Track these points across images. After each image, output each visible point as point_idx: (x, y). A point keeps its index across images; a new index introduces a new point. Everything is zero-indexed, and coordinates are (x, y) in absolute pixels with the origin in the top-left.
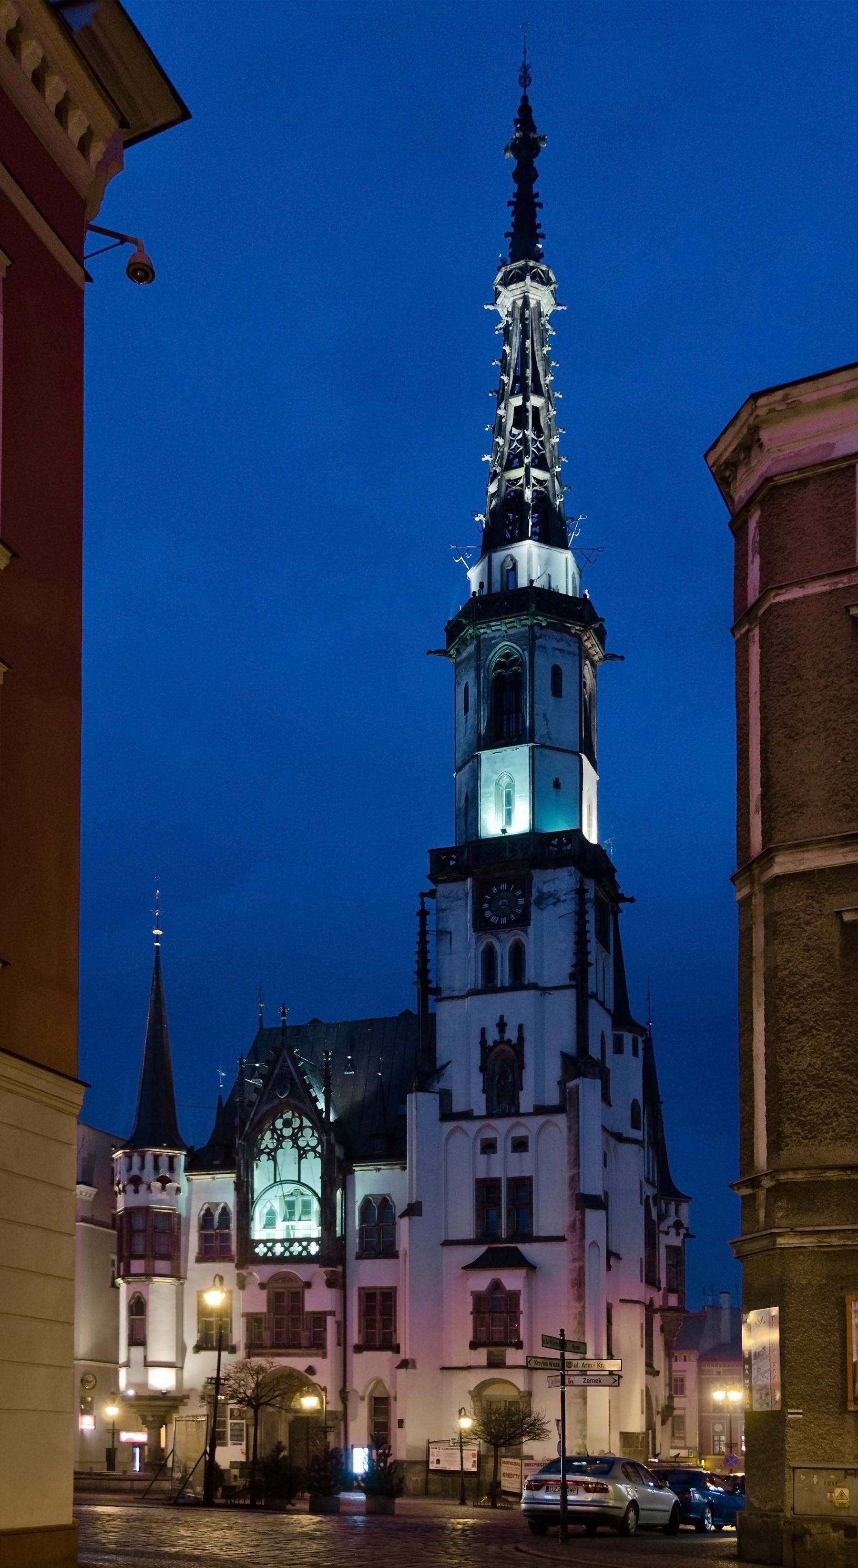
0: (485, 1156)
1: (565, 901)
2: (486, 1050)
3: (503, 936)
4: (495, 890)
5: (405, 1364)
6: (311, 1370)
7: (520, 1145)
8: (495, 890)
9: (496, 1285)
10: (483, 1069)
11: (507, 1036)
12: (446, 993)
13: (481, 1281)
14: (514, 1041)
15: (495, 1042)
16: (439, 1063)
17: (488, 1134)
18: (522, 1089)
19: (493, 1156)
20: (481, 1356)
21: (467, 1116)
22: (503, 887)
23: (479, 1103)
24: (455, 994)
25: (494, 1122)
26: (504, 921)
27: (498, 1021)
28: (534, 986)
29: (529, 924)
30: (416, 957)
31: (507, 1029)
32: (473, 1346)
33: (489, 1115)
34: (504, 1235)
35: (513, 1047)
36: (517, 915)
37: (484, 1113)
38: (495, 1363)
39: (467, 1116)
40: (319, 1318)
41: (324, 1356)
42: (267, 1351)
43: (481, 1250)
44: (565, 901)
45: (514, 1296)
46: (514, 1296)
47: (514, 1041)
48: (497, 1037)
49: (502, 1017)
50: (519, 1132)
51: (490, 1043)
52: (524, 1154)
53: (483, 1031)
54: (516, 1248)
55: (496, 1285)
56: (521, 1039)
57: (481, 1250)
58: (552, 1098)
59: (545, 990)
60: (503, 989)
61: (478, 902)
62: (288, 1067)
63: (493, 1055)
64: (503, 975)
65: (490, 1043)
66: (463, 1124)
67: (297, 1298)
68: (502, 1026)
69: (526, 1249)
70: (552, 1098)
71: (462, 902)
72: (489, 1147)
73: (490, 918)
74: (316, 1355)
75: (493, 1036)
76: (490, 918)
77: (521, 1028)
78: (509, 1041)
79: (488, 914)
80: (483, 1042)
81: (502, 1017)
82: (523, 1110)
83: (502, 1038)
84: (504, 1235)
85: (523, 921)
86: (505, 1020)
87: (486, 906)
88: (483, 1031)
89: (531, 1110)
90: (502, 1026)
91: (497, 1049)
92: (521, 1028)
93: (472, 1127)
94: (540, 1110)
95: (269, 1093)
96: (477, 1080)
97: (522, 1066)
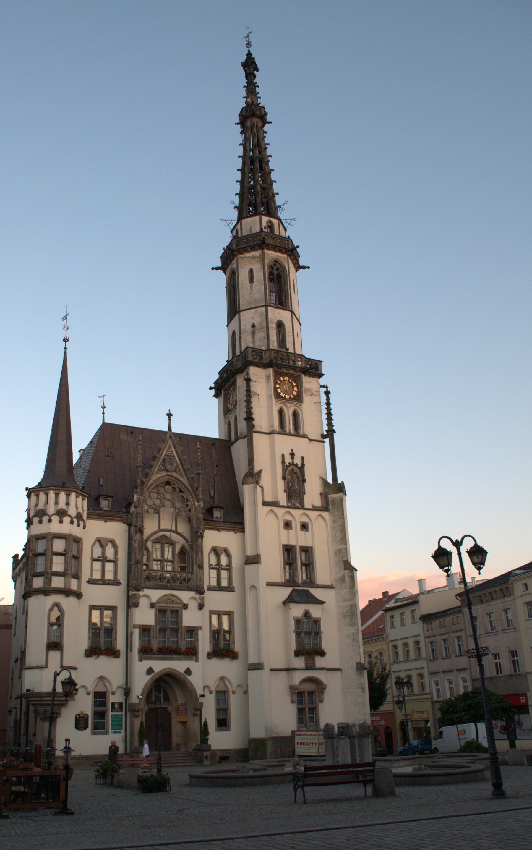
0: (286, 531)
1: (316, 395)
2: (285, 467)
3: (289, 405)
4: (282, 379)
5: (258, 667)
6: (188, 671)
7: (304, 527)
8: (282, 379)
9: (307, 614)
10: (284, 478)
11: (295, 463)
12: (257, 429)
13: (297, 610)
14: (299, 465)
15: (289, 463)
16: (256, 469)
17: (288, 518)
18: (305, 493)
19: (290, 531)
20: (300, 662)
21: (275, 504)
22: (286, 378)
23: (283, 498)
24: (263, 431)
25: (292, 511)
26: (287, 397)
27: (290, 452)
28: (304, 436)
29: (302, 402)
30: (245, 404)
31: (295, 457)
32: (297, 654)
33: (288, 507)
34: (300, 581)
35: (299, 468)
36: (294, 396)
37: (285, 504)
38: (310, 667)
39: (275, 504)
40: (193, 631)
41: (197, 660)
42: (155, 656)
43: (288, 590)
44: (316, 395)
45: (317, 622)
46: (317, 622)
47: (299, 465)
48: (290, 461)
49: (292, 450)
50: (305, 519)
51: (287, 464)
52: (306, 532)
53: (283, 455)
54: (308, 591)
55: (307, 614)
56: (303, 465)
57: (289, 590)
58: (318, 503)
59: (310, 440)
60: (290, 434)
61: (275, 383)
62: (172, 452)
63: (288, 471)
64: (290, 426)
65: (287, 464)
66: (275, 509)
67: (176, 613)
68: (292, 455)
69: (315, 592)
70: (318, 503)
71: (264, 380)
72: (288, 525)
73: (280, 393)
74: (191, 659)
75: (288, 460)
76: (280, 393)
77: (303, 458)
78: (296, 465)
79: (279, 390)
80: (283, 462)
81: (292, 450)
82: (306, 506)
83: (293, 462)
84: (300, 581)
85: (298, 398)
86: (294, 451)
87: (278, 386)
88: (283, 455)
89: (310, 507)
90: (292, 455)
91: (290, 468)
92: (303, 458)
93: (280, 511)
94: (315, 509)
95: (159, 467)
96: (281, 485)
97: (304, 481)
